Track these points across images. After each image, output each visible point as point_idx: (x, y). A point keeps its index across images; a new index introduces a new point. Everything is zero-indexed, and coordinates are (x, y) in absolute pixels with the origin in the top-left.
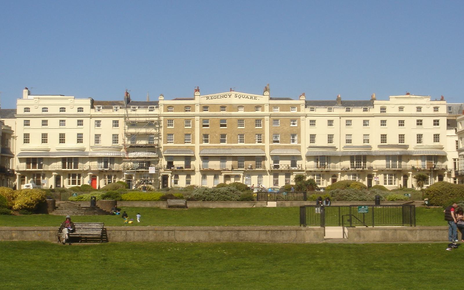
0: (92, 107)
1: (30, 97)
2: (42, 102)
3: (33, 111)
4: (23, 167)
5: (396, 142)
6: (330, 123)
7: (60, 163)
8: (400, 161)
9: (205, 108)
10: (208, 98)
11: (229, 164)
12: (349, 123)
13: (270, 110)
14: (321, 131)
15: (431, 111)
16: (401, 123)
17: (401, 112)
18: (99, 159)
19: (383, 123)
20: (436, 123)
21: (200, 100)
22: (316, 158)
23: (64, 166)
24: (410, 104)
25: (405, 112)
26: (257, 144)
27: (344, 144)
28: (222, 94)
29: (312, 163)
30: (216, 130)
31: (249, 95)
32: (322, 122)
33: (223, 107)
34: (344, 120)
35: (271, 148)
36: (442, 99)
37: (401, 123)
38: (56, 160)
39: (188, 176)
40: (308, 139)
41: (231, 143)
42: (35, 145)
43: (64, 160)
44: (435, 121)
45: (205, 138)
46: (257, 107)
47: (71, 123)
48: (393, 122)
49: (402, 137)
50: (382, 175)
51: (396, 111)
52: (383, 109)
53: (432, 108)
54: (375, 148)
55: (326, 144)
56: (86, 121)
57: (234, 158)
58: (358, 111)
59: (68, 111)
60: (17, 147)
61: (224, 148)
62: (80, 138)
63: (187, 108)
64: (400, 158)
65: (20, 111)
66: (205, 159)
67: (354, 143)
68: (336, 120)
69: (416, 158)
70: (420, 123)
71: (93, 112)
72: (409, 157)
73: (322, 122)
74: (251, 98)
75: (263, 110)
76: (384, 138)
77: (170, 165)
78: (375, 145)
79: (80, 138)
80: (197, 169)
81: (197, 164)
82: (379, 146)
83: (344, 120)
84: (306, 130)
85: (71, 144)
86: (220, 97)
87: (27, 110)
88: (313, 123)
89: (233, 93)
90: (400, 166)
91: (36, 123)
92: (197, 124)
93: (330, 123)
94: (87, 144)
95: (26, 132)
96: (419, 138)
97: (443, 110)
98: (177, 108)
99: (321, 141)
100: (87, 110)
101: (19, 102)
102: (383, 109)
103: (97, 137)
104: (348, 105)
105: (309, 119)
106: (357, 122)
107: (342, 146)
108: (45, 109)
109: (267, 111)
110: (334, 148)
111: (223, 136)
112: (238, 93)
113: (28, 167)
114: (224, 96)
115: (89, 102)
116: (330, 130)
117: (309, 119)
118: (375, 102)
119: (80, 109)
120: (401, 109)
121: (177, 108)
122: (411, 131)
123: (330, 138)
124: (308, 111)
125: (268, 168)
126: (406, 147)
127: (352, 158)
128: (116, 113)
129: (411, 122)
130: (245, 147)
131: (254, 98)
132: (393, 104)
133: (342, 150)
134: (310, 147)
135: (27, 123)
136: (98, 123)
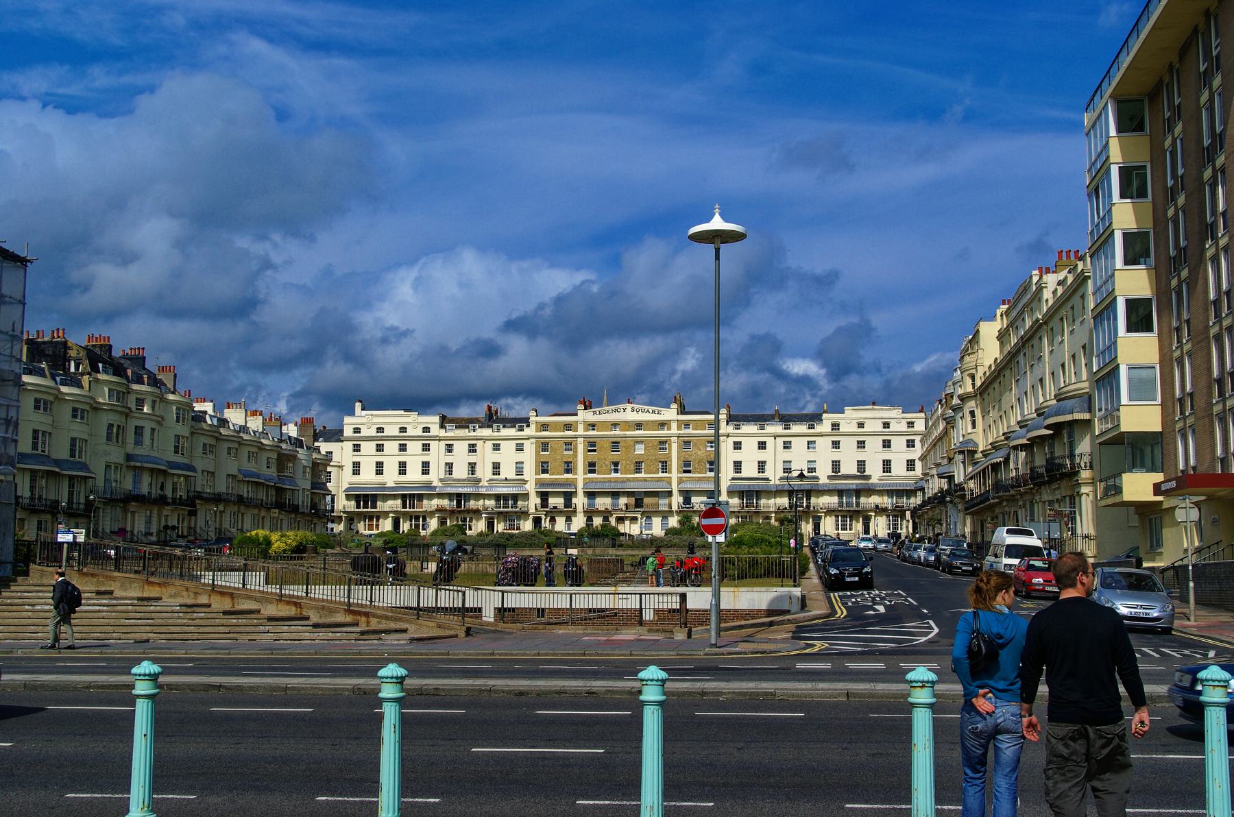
0: (442, 426)
1: (364, 412)
2: (376, 420)
3: (365, 432)
4: (351, 506)
5: (853, 470)
6: (762, 445)
7: (399, 502)
8: (858, 497)
9: (592, 426)
10: (595, 413)
11: (623, 501)
12: (787, 446)
14: (750, 456)
15: (903, 427)
16: (861, 445)
17: (861, 430)
18: (450, 496)
19: (836, 445)
20: (910, 444)
21: (584, 415)
22: (741, 494)
23: (404, 506)
24: (873, 418)
25: (866, 429)
26: (661, 475)
27: (780, 474)
28: (614, 407)
29: (735, 501)
30: (605, 456)
31: (651, 408)
32: (750, 445)
33: (615, 425)
34: (780, 441)
35: (680, 481)
36: (921, 411)
37: (861, 445)
38: (394, 497)
39: (569, 520)
40: (731, 467)
42: (368, 476)
43: (404, 497)
44: (908, 441)
45: (591, 467)
46: (663, 425)
47: (414, 447)
48: (848, 444)
49: (861, 464)
50: (833, 518)
51: (855, 429)
52: (835, 426)
53: (904, 423)
54: (823, 480)
55: (755, 474)
56: (433, 444)
57: (629, 494)
58: (797, 428)
59: (410, 432)
60: (340, 482)
61: (616, 481)
62: (426, 468)
63: (568, 427)
64: (858, 493)
65: (348, 431)
66: (591, 495)
68: (770, 442)
69: (880, 493)
70: (887, 444)
71: (442, 433)
72: (870, 491)
73: (750, 445)
74: (654, 412)
75: (669, 429)
76: (836, 465)
77: (544, 503)
78: (823, 474)
79: (426, 468)
80: (580, 509)
81: (580, 501)
82: (829, 477)
83: (780, 441)
84: (728, 456)
85: (414, 475)
87: (357, 430)
88: (737, 446)
89: (629, 407)
90: (858, 504)
91: (368, 448)
92: (581, 448)
93: (762, 445)
94: (435, 477)
95: (356, 459)
96: (887, 466)
97: (920, 426)
98: (556, 426)
99: (750, 470)
100: (435, 430)
101: (347, 420)
102: (835, 426)
103: (450, 466)
104: (787, 420)
105: (731, 440)
106: (799, 444)
107: (778, 477)
108: (380, 430)
109: (674, 430)
110: (767, 479)
111: (616, 464)
112: (636, 406)
113: (358, 506)
114: (616, 411)
115: (436, 419)
116: (762, 456)
117: (731, 440)
118: (824, 416)
119: (426, 430)
120: (861, 425)
121: (556, 426)
122: (874, 457)
123: (762, 465)
124: (730, 429)
125: (675, 507)
126: (869, 477)
127: (791, 493)
128: (472, 434)
129: (874, 444)
130: (645, 480)
132: (849, 418)
133: (778, 482)
134: (733, 479)
135: (357, 448)
136: (449, 449)
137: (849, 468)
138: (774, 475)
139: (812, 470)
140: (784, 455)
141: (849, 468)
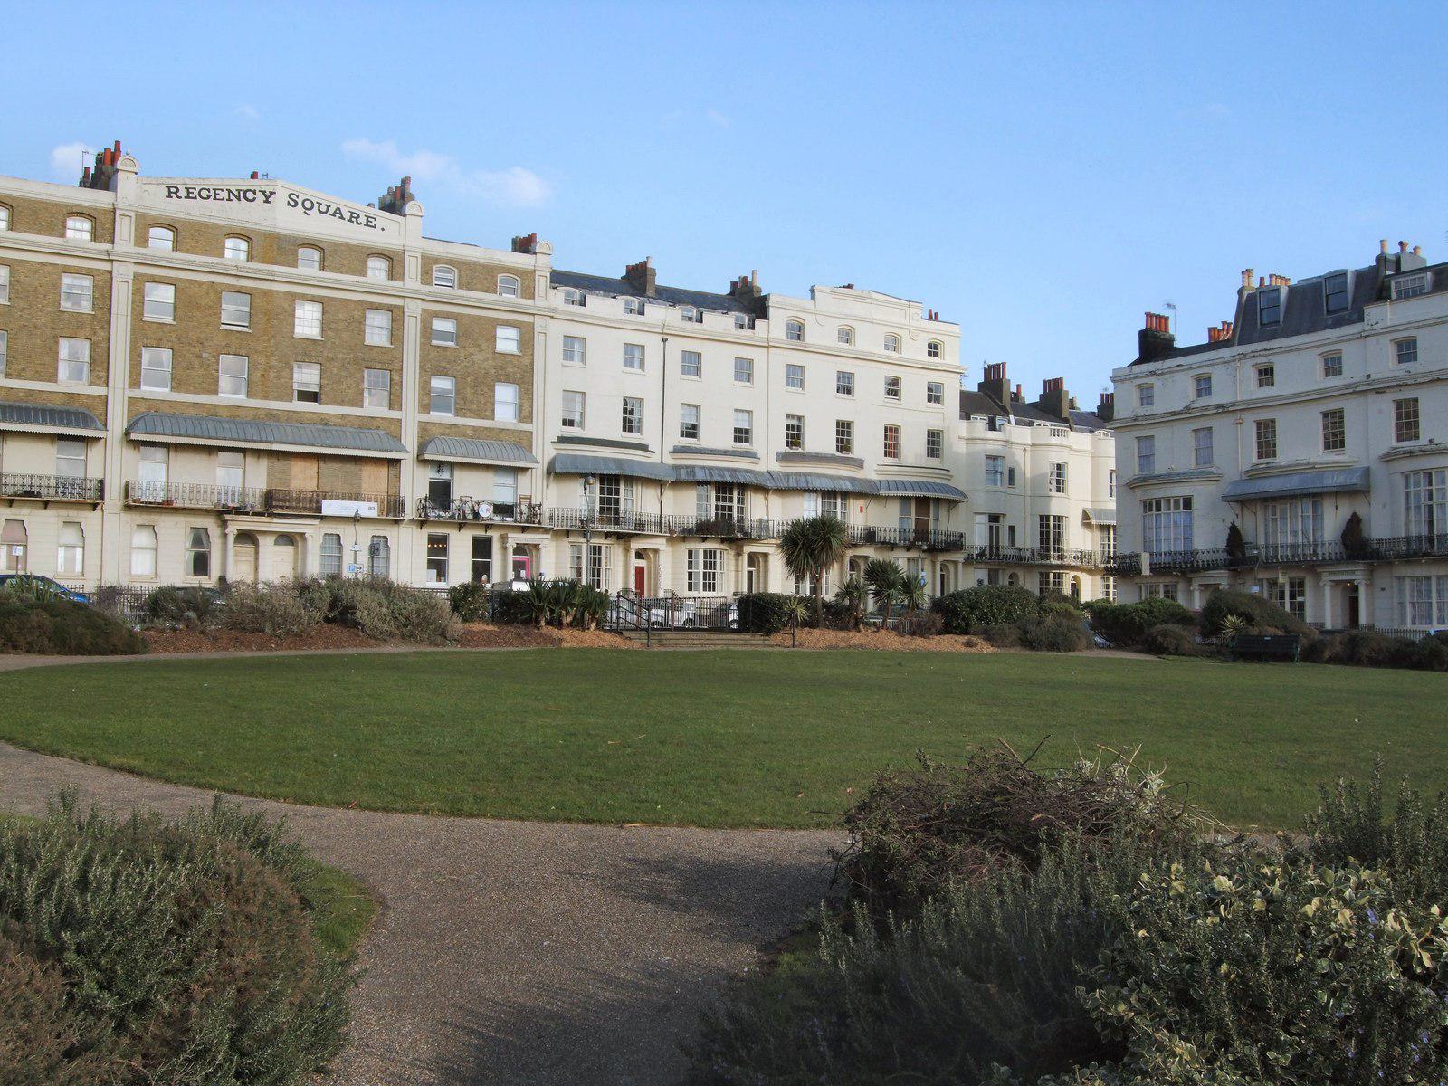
6: (633, 355)
13: (427, 276)
27: (674, 439)
29: (578, 500)
32: (605, 347)
41: (266, 398)
49: (844, 429)
55: (618, 434)
67: (707, 439)
68: (652, 344)
82: (783, 457)
83: (676, 347)
86: (225, 195)
102: (797, 331)
106: (719, 361)
107: (668, 447)
110: (644, 448)
126: (859, 464)
131: (363, 220)
133: (669, 460)
134: (563, 440)
137: (820, 439)
138: (659, 442)
139: (742, 435)
140: (685, 389)
141: (820, 439)
